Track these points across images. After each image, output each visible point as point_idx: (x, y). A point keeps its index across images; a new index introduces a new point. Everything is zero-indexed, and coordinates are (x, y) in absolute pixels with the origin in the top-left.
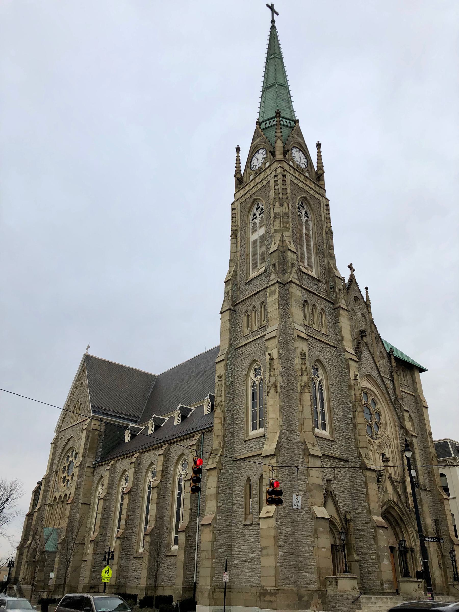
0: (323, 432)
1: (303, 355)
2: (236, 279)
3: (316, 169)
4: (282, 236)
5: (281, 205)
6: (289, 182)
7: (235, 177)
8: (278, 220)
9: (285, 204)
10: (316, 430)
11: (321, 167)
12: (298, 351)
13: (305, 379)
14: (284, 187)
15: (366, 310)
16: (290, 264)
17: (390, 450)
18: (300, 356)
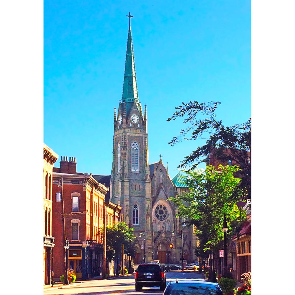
0: (137, 224)
1: (127, 205)
2: (114, 171)
3: (143, 119)
4: (123, 163)
5: (124, 149)
6: (128, 137)
7: (114, 124)
8: (123, 156)
9: (125, 149)
10: (134, 224)
11: (145, 118)
12: (126, 204)
13: (127, 213)
14: (125, 141)
15: (165, 173)
16: (125, 174)
17: (170, 223)
18: (126, 206)
